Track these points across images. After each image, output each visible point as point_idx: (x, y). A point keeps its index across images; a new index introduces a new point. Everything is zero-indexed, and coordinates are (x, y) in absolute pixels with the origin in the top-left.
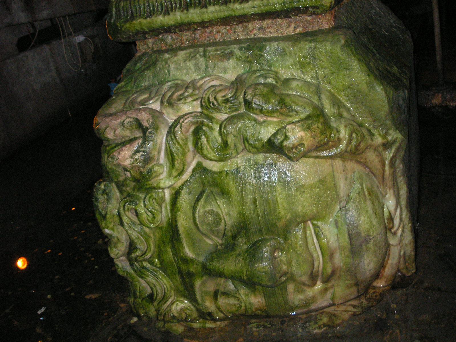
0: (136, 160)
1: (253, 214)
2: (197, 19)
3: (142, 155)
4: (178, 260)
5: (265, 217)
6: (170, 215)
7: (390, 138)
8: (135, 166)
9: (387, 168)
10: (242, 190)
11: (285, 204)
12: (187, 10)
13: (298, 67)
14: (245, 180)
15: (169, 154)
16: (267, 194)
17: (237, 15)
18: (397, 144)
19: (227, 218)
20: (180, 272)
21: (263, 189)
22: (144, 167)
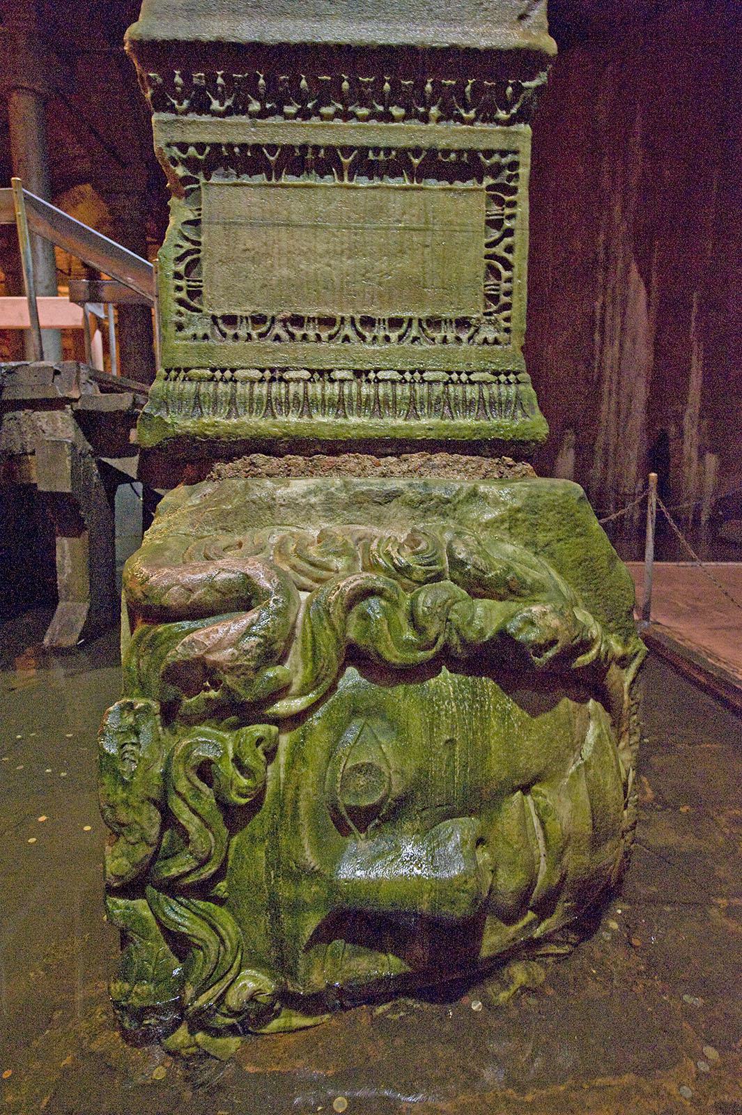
0: (247, 652)
1: (445, 772)
2: (326, 435)
3: (259, 645)
4: (277, 876)
5: (466, 777)
6: (282, 776)
7: (629, 650)
8: (240, 666)
9: (626, 697)
10: (431, 724)
11: (500, 753)
12: (310, 416)
13: (506, 525)
14: (438, 706)
15: (309, 646)
16: (475, 733)
17: (398, 437)
18: (637, 661)
19: (396, 778)
20: (273, 905)
21: (470, 724)
22: (257, 669)
